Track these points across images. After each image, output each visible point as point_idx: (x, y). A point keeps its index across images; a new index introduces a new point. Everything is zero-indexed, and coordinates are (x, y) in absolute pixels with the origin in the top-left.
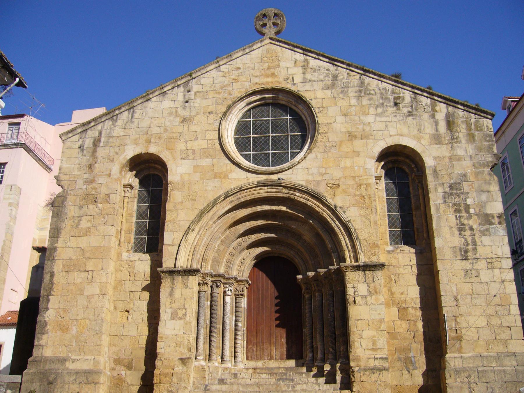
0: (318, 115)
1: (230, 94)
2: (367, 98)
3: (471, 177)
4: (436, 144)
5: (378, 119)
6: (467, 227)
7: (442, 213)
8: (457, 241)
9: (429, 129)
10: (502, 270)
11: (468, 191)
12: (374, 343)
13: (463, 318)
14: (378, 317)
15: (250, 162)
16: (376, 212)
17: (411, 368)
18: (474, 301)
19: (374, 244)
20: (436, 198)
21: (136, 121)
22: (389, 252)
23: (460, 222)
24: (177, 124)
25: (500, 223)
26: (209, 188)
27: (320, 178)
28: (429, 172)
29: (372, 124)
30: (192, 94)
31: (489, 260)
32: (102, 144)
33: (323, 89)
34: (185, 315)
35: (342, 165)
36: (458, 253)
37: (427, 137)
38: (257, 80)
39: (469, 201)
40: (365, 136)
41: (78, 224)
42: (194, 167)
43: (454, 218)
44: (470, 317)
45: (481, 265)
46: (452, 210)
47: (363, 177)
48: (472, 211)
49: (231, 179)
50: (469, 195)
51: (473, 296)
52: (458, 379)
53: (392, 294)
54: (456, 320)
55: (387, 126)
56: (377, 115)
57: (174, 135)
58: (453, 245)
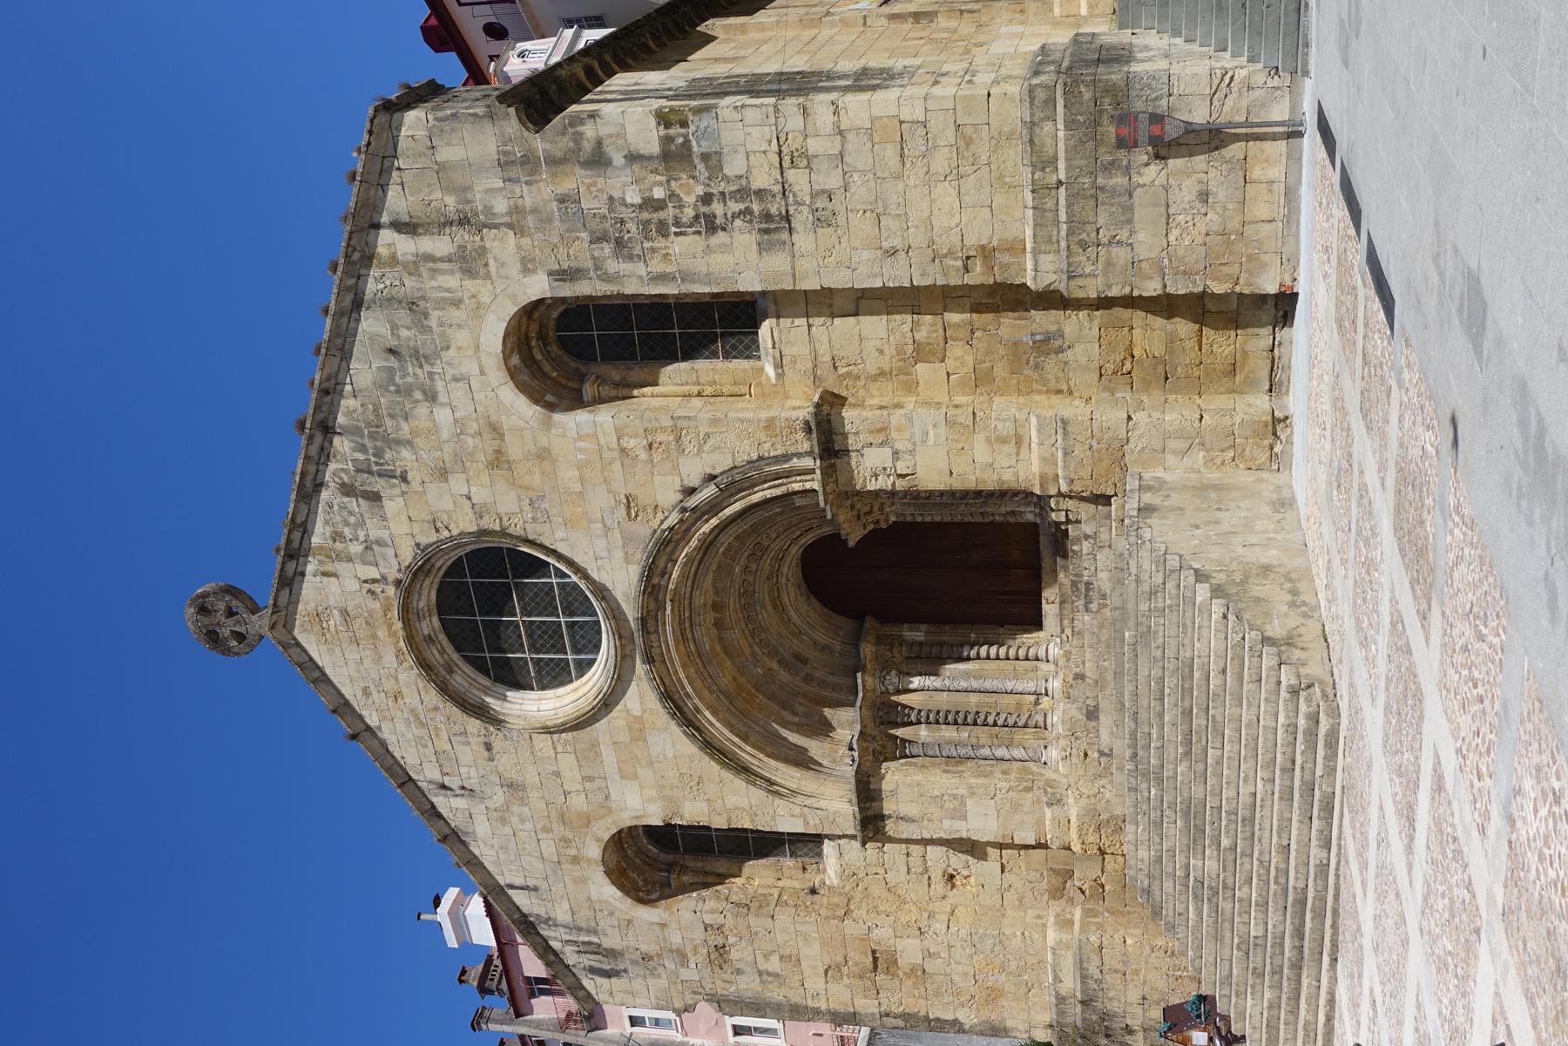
0: (455, 532)
1: (436, 709)
2: (388, 422)
3: (567, 185)
4: (486, 265)
5: (442, 398)
6: (704, 209)
7: (671, 269)
8: (744, 239)
9: (451, 281)
10: (810, 130)
11: (605, 196)
12: (1003, 440)
13: (937, 240)
14: (942, 429)
15: (591, 663)
16: (688, 418)
17: (1058, 343)
18: (893, 209)
19: (767, 428)
20: (635, 279)
21: (531, 883)
22: (780, 376)
23: (690, 226)
24: (526, 809)
25: (684, 124)
26: (670, 755)
27: (617, 535)
28: (567, 291)
29: (458, 415)
30: (447, 781)
31: (786, 164)
32: (595, 940)
33: (384, 518)
34: (955, 796)
35: (577, 487)
36: (775, 237)
37: (468, 283)
38: (390, 659)
39: (634, 197)
40: (496, 431)
41: (777, 975)
42: (622, 777)
43: (681, 238)
44: (936, 223)
45: (798, 179)
46: (660, 243)
47: (602, 442)
48: (658, 193)
49: (644, 711)
50: (616, 194)
51: (880, 210)
52: (1087, 271)
53: (882, 373)
54: (945, 256)
55: (456, 379)
56: (432, 397)
57: (554, 814)
58: (755, 248)
